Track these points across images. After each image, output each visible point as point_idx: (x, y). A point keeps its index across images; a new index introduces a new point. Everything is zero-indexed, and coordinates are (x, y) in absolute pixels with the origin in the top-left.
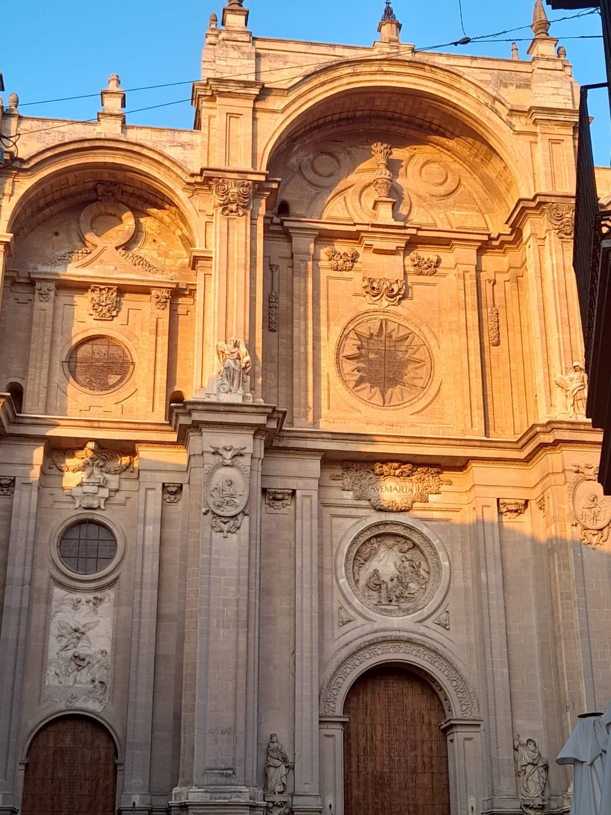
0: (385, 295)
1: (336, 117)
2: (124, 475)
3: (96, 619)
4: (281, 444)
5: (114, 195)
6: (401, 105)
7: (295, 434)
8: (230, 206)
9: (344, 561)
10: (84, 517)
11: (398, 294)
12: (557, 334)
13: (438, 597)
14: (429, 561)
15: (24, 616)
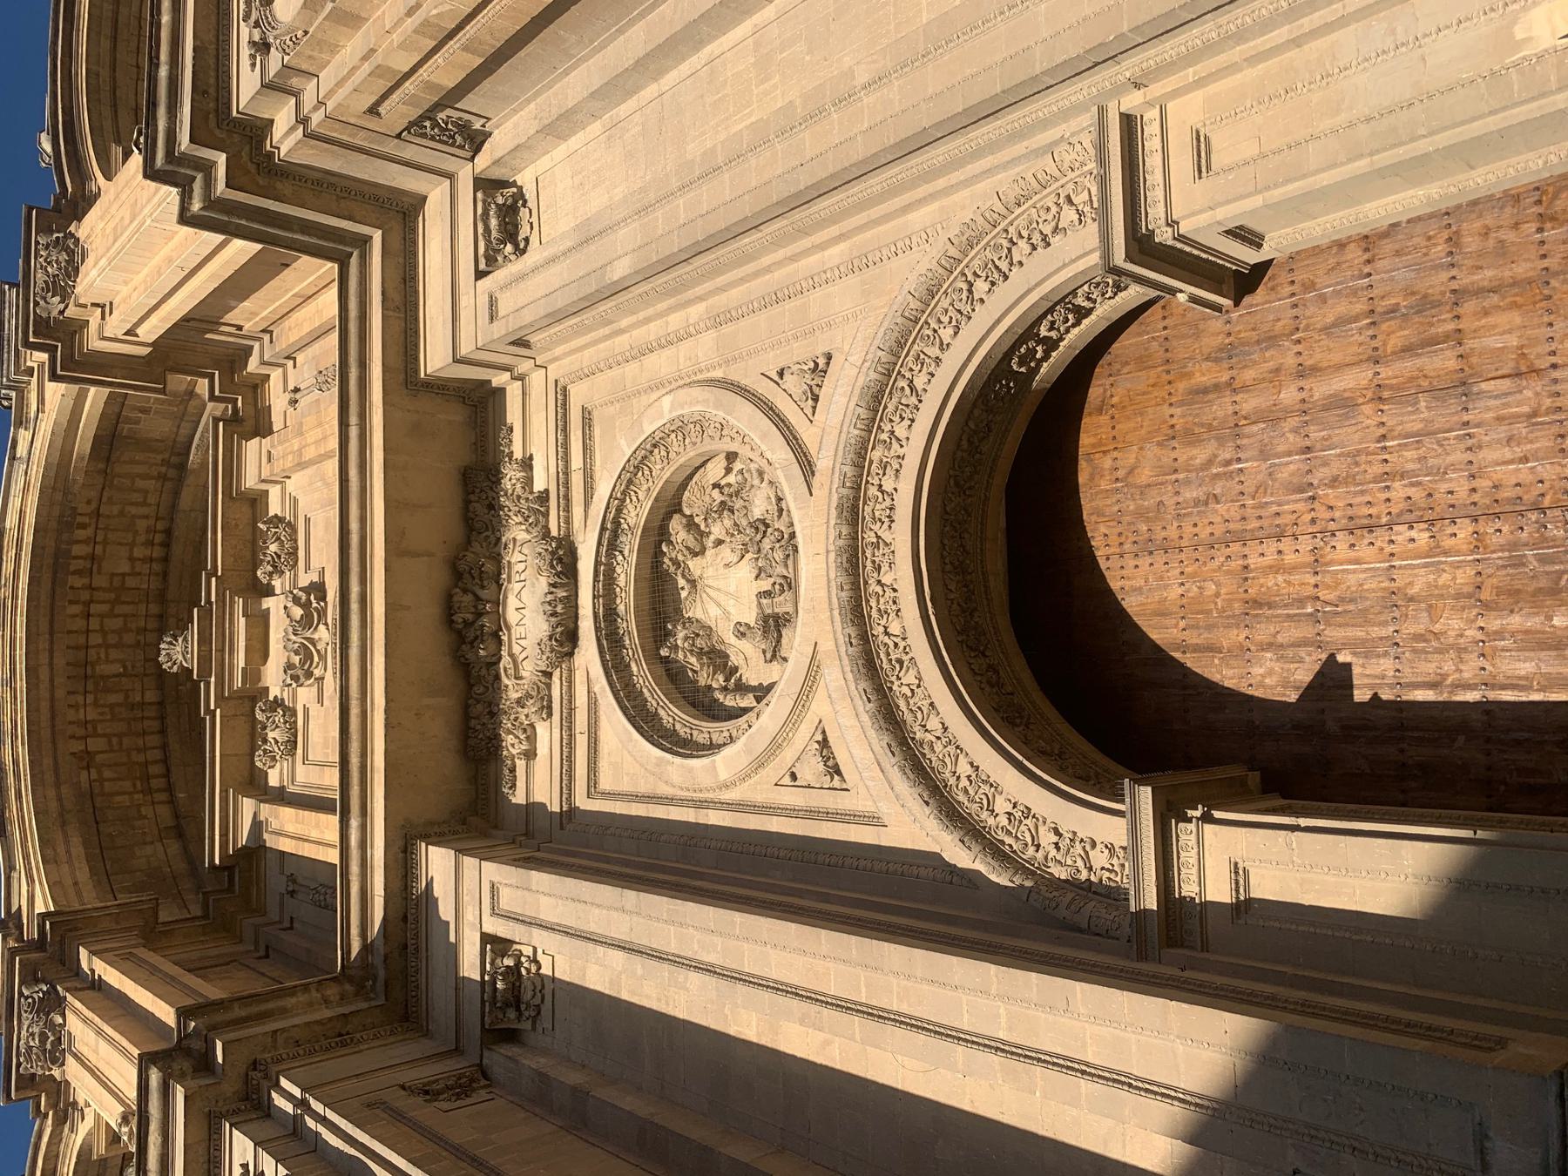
0: (308, 634)
1: (154, 740)
4: (382, 974)
6: (116, 623)
8: (48, 1046)
9: (678, 760)
11: (306, 606)
12: (148, 222)
13: (745, 417)
14: (682, 460)
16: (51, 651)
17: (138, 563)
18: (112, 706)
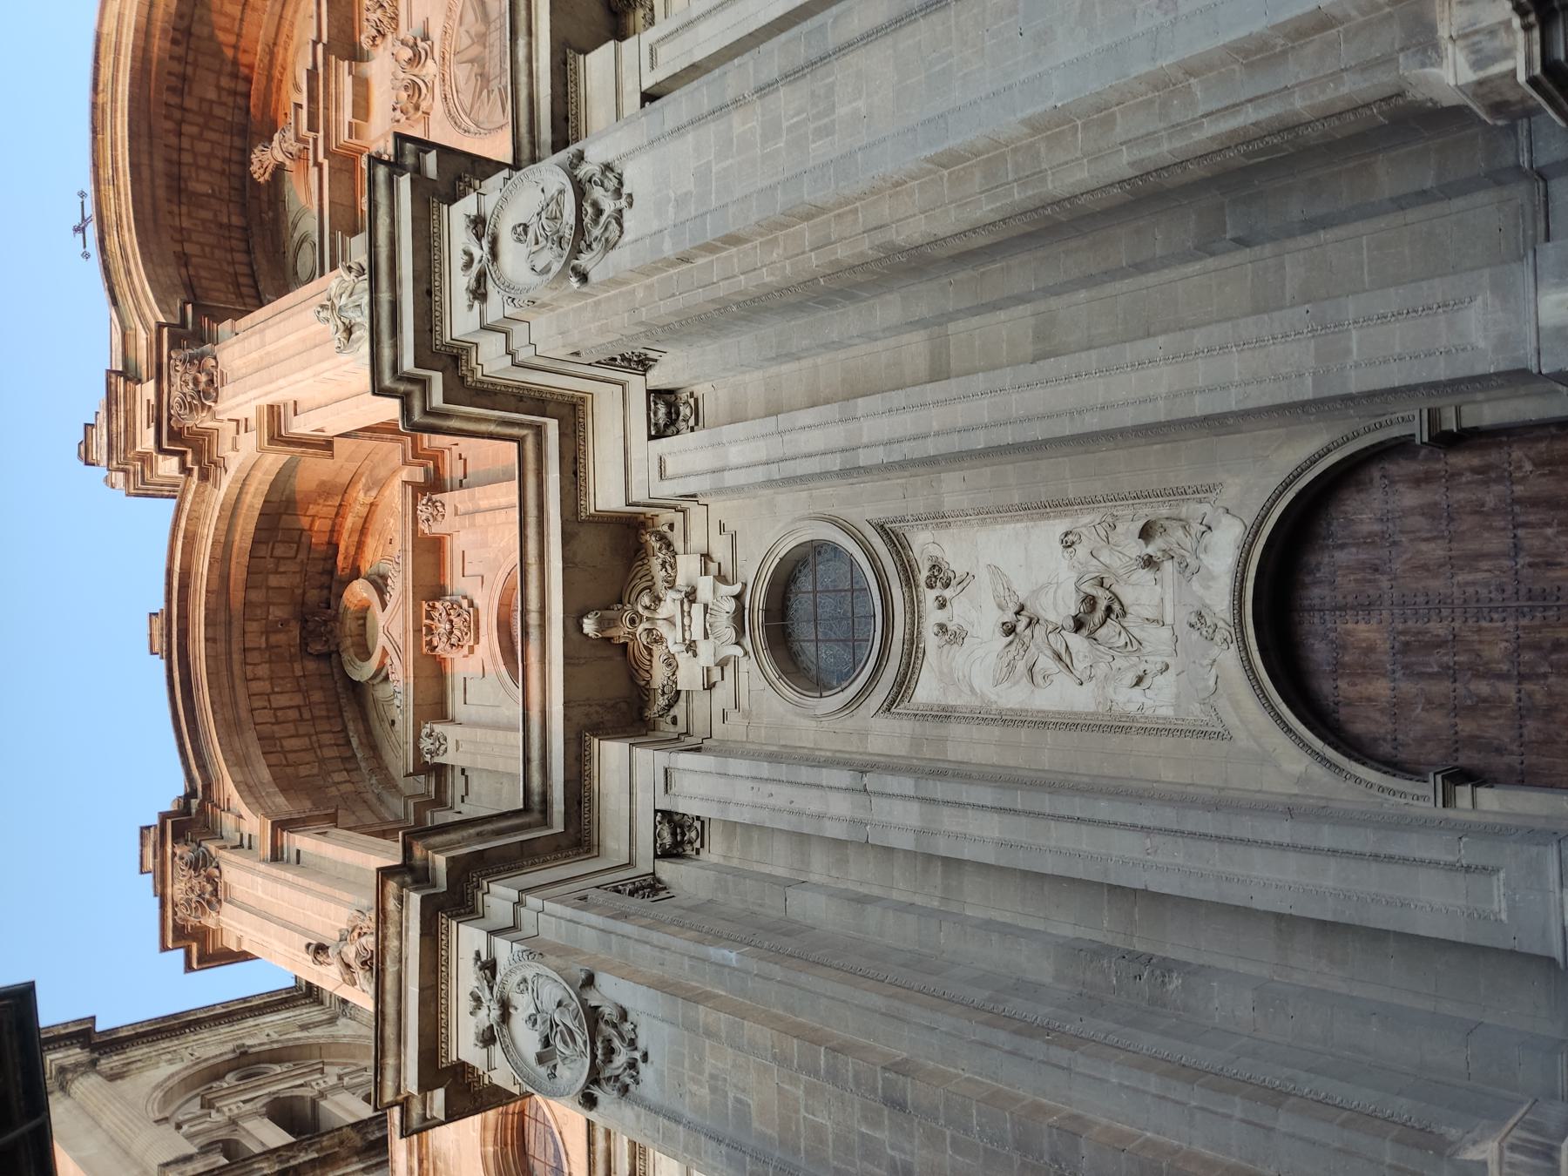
0: (416, 71)
1: (240, 257)
2: (678, 545)
3: (984, 577)
5: (325, 623)
6: (204, 147)
7: (524, 129)
8: (202, 386)
10: (759, 634)
15: (939, 789)
16: (151, 154)
17: (224, 93)
18: (204, 221)
